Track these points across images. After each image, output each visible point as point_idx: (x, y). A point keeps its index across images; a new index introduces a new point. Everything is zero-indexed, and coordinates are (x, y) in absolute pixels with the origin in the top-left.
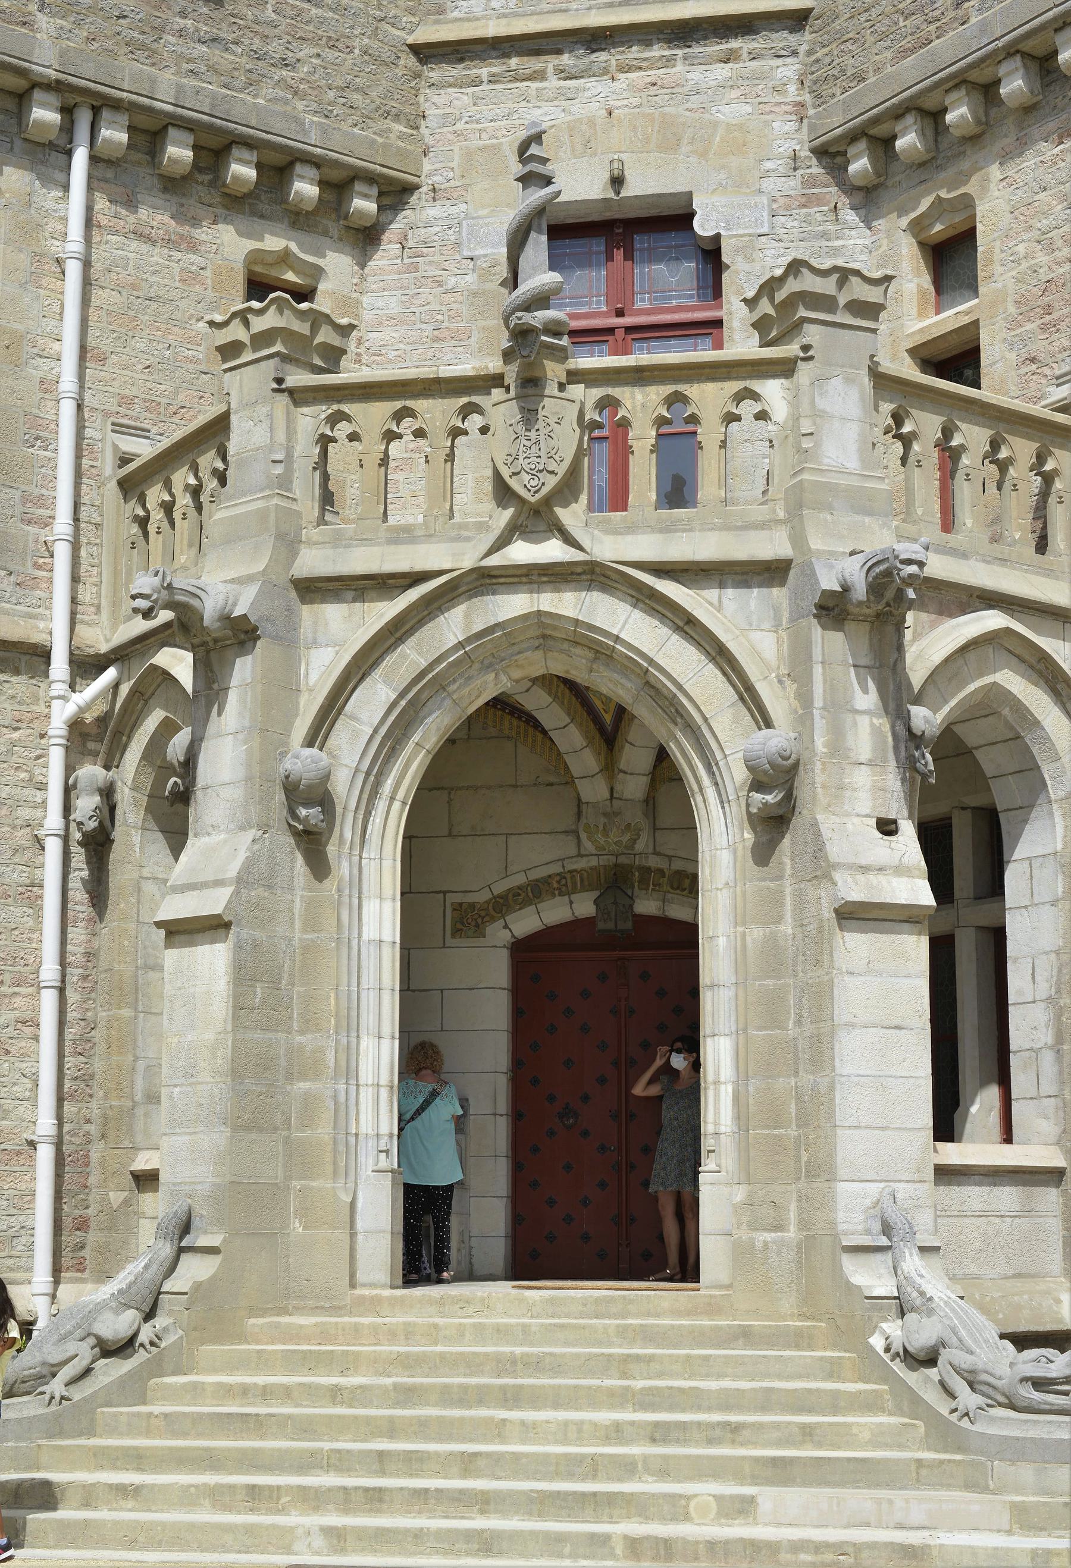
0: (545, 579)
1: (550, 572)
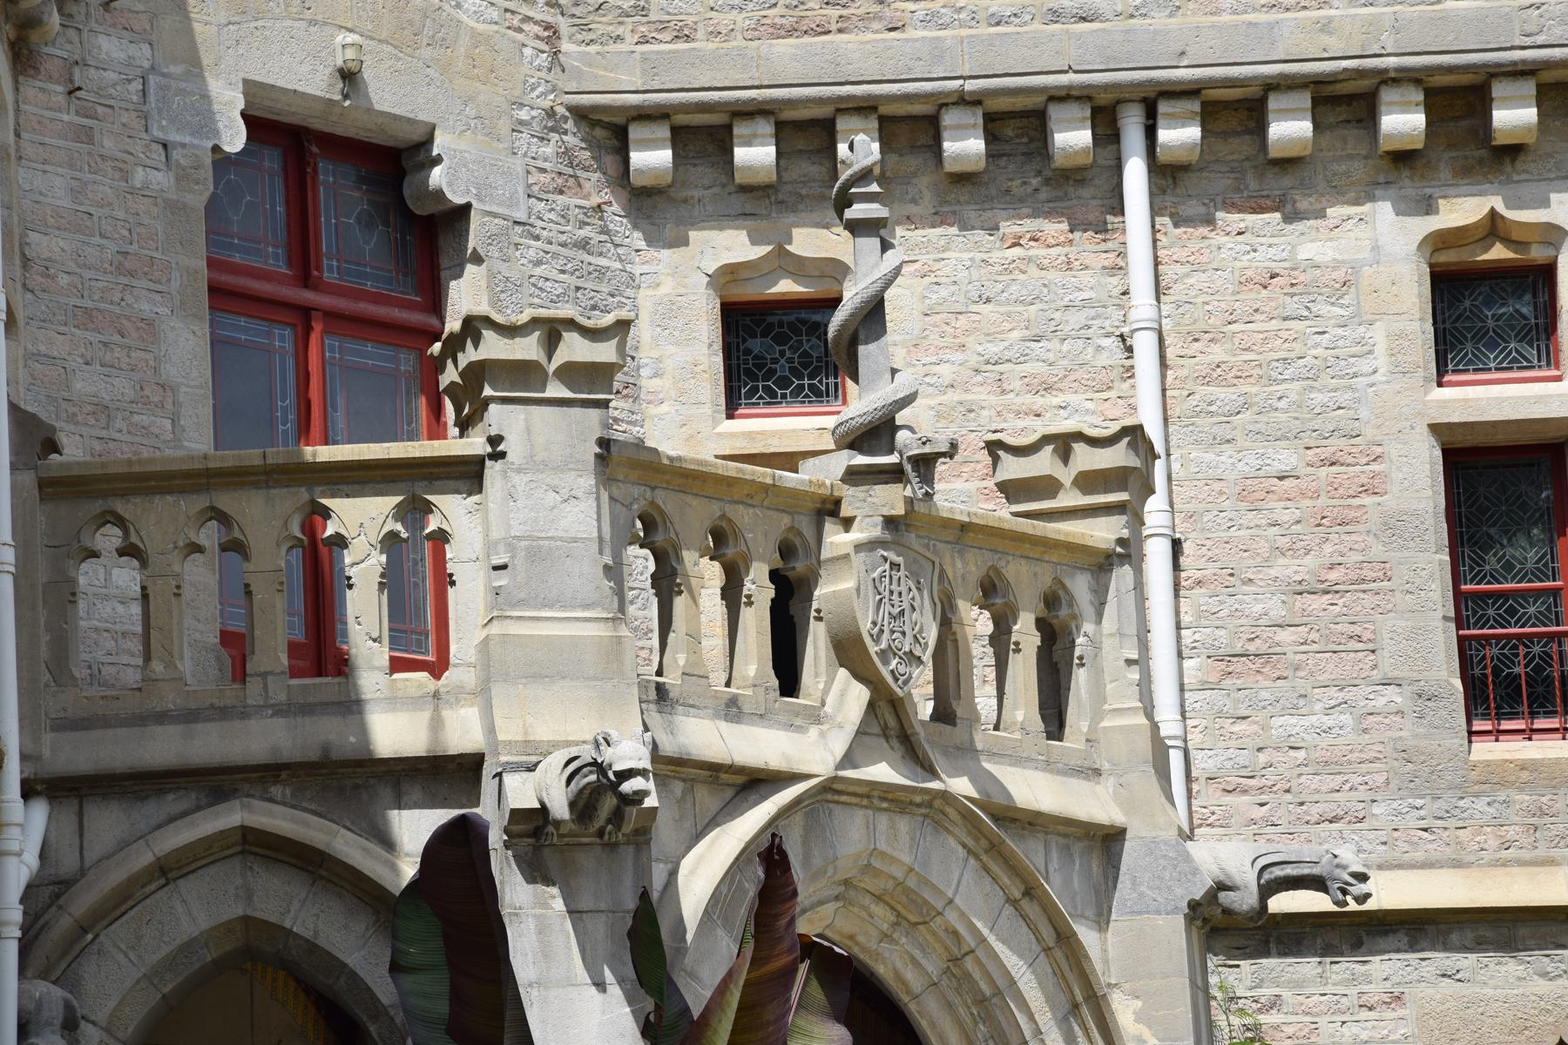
0: (885, 805)
1: (890, 796)
